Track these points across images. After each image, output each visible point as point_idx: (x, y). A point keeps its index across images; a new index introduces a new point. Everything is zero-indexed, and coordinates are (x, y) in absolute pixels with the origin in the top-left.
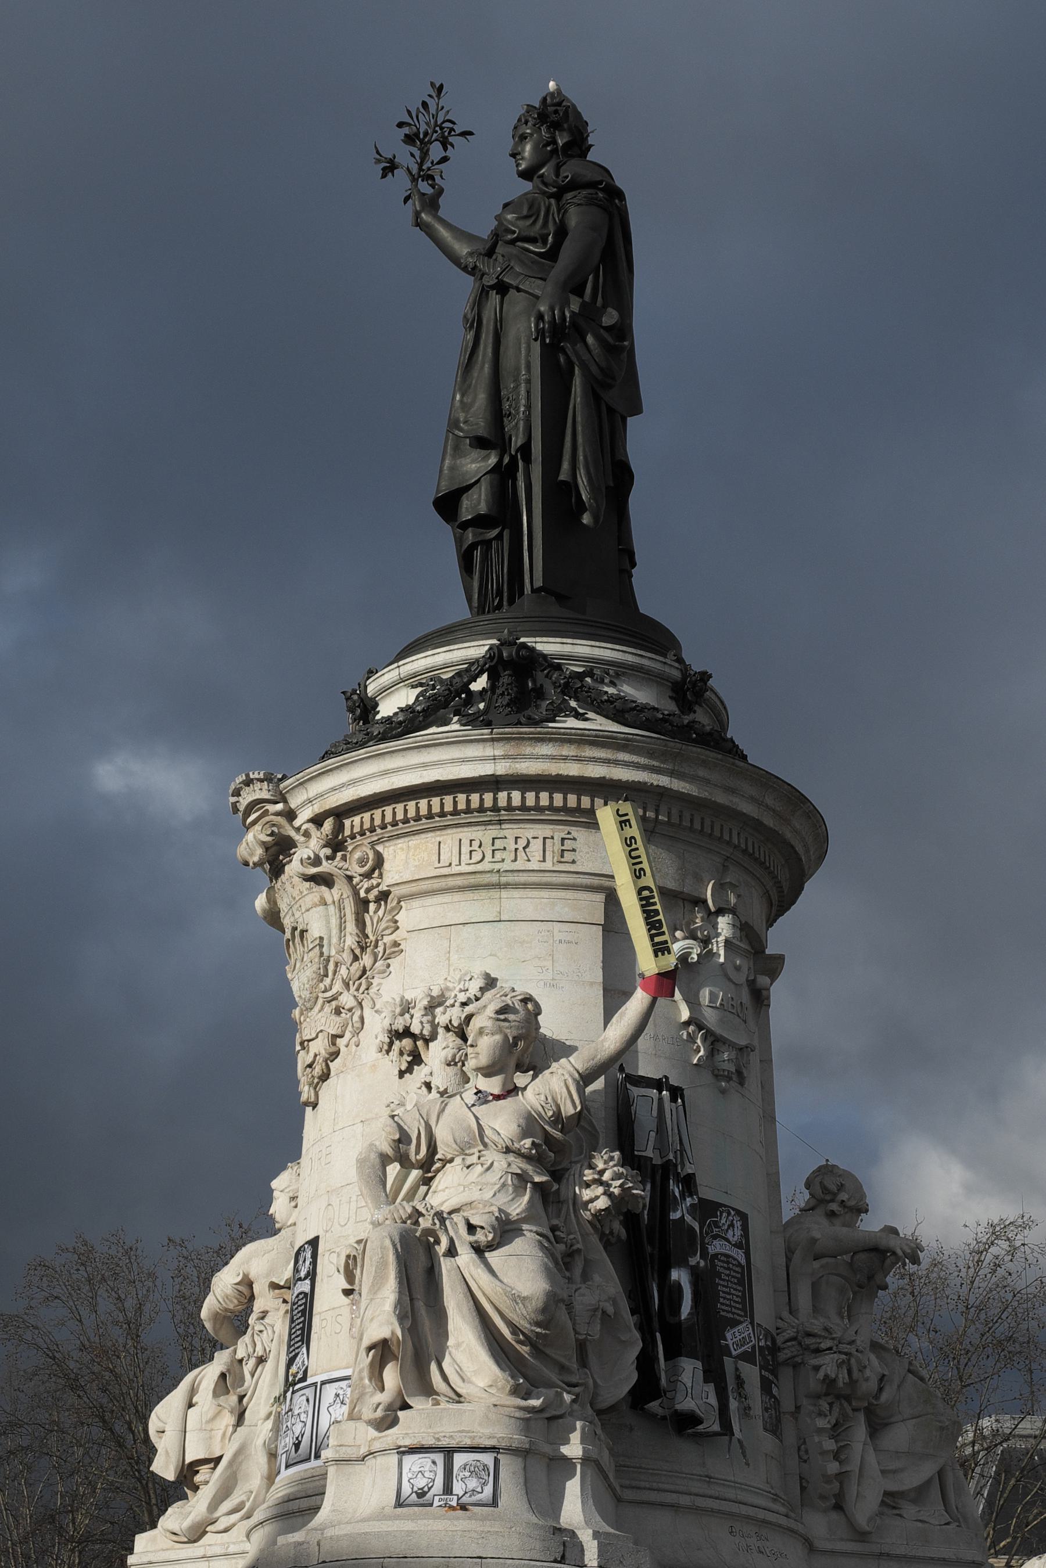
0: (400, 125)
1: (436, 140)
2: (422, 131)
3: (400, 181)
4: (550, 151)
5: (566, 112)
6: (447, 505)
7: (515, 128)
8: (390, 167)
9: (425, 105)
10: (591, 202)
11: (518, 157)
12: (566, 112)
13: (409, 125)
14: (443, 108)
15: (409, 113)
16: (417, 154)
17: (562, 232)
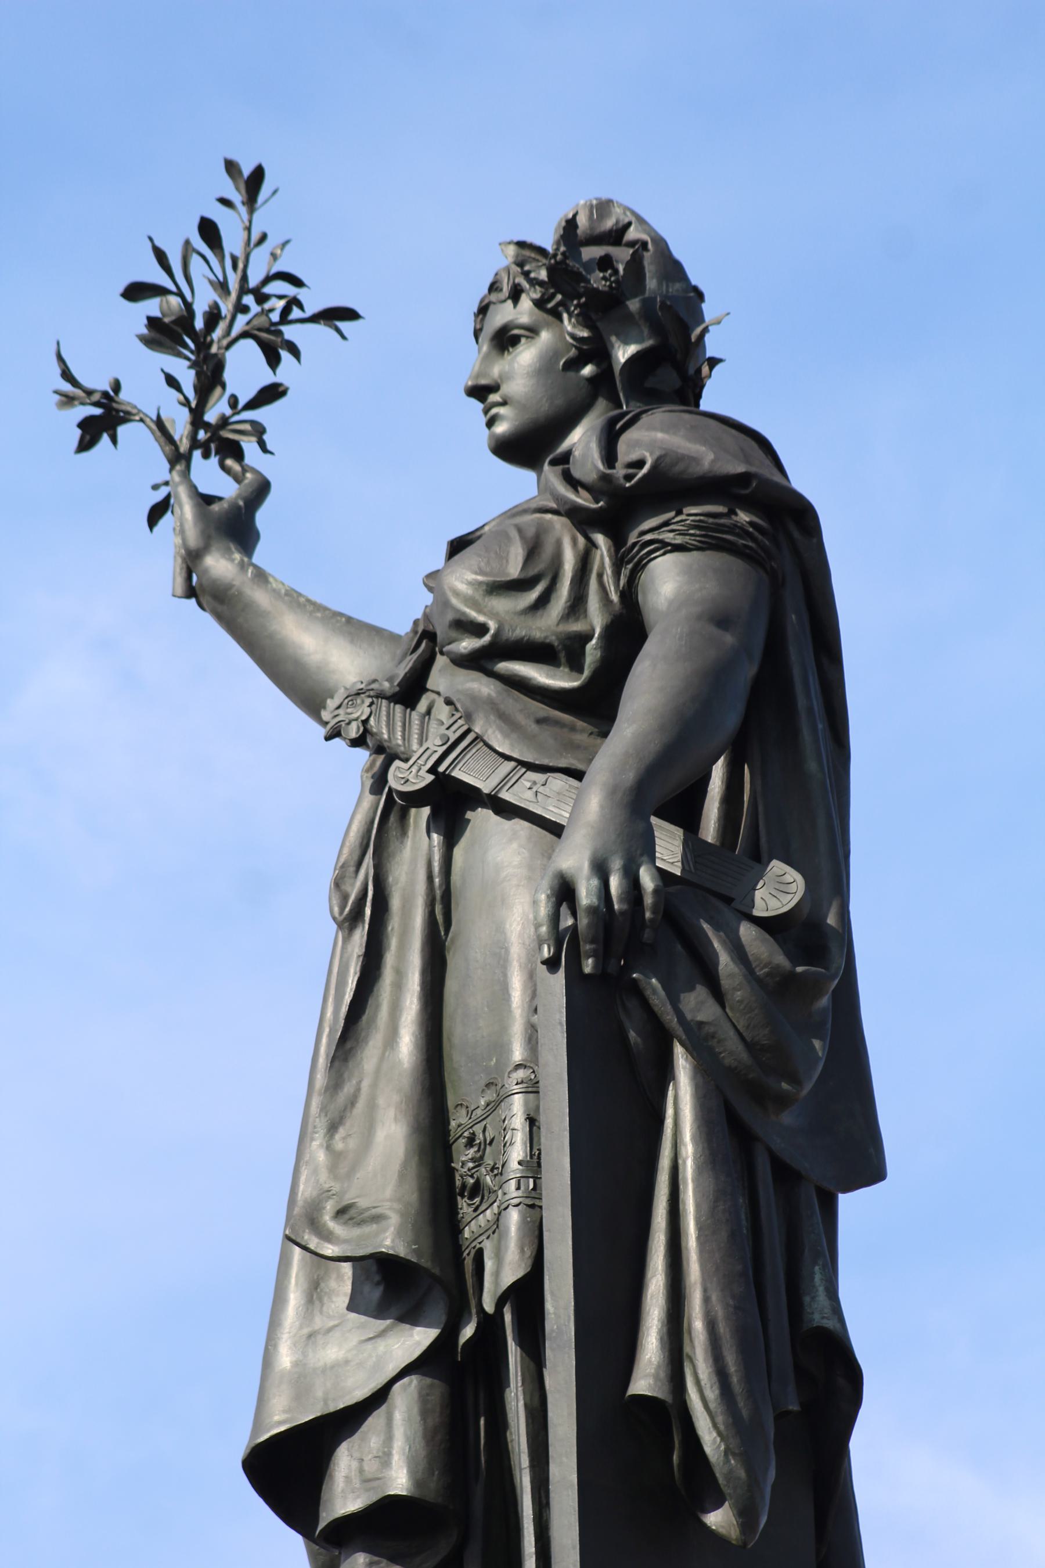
0: (136, 292)
1: (245, 335)
2: (200, 308)
3: (136, 459)
4: (591, 380)
5: (635, 264)
6: (287, 1469)
7: (483, 310)
8: (105, 419)
9: (209, 230)
10: (711, 539)
11: (494, 398)
12: (635, 264)
13: (157, 291)
14: (263, 238)
15: (161, 257)
16: (187, 378)
17: (628, 630)
